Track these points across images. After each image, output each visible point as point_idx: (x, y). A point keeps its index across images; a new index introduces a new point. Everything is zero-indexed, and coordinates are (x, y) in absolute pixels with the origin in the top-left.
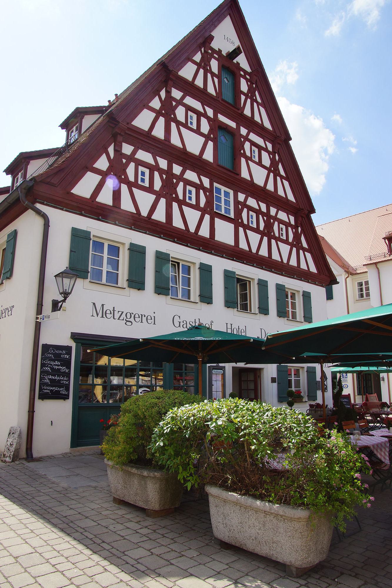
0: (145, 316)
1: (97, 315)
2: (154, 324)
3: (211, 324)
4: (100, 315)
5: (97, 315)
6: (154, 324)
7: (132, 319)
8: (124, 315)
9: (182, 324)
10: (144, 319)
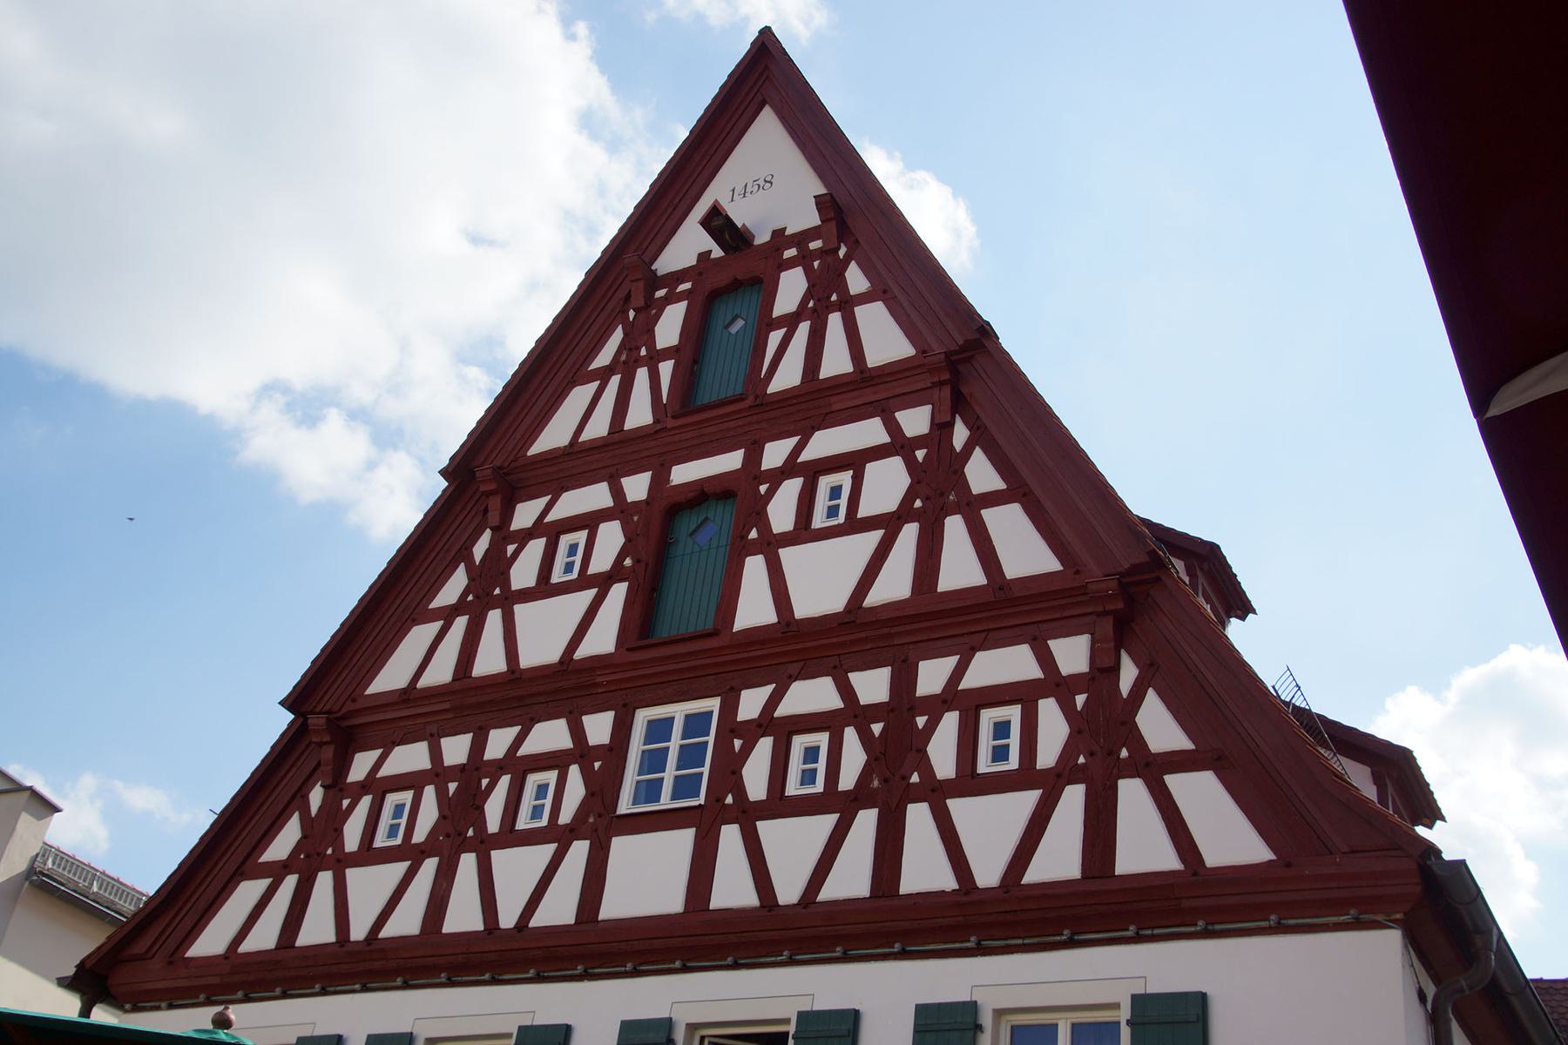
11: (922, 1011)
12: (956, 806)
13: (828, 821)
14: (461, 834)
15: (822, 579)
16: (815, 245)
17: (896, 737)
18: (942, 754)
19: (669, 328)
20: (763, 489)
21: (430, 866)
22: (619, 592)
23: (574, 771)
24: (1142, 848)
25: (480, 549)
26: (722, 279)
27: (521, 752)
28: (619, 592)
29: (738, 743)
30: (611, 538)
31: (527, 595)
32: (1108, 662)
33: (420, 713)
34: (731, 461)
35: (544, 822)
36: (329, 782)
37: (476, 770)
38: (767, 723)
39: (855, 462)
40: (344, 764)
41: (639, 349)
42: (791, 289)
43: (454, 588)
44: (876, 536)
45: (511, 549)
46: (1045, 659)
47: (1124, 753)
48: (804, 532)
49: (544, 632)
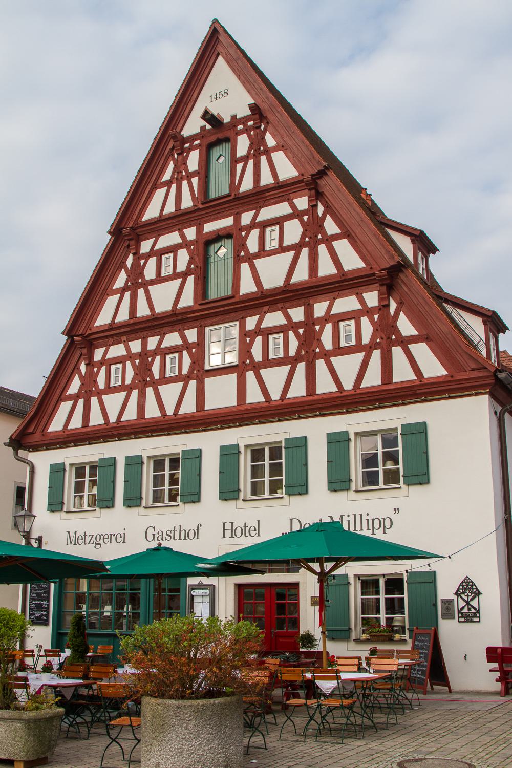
0: (114, 535)
1: (71, 542)
2: (124, 542)
3: (198, 529)
4: (73, 543)
5: (71, 542)
6: (124, 542)
7: (101, 542)
8: (94, 539)
9: (156, 536)
10: (113, 538)
11: (329, 435)
12: (333, 360)
13: (287, 368)
14: (144, 380)
15: (273, 272)
16: (251, 123)
17: (309, 333)
18: (327, 341)
19: (193, 161)
20: (243, 234)
21: (135, 393)
22: (191, 279)
23: (185, 353)
24: (402, 373)
25: (129, 261)
26: (213, 139)
27: (162, 346)
28: (191, 279)
29: (248, 339)
30: (183, 257)
31: (152, 282)
32: (385, 303)
34: (228, 222)
35: (177, 373)
36: (87, 362)
37: (144, 354)
38: (258, 331)
39: (279, 221)
40: (91, 356)
41: (181, 172)
42: (243, 144)
43: (121, 280)
44: (292, 253)
45: (142, 262)
46: (362, 301)
47: (394, 337)
48: (263, 252)
49: (164, 297)
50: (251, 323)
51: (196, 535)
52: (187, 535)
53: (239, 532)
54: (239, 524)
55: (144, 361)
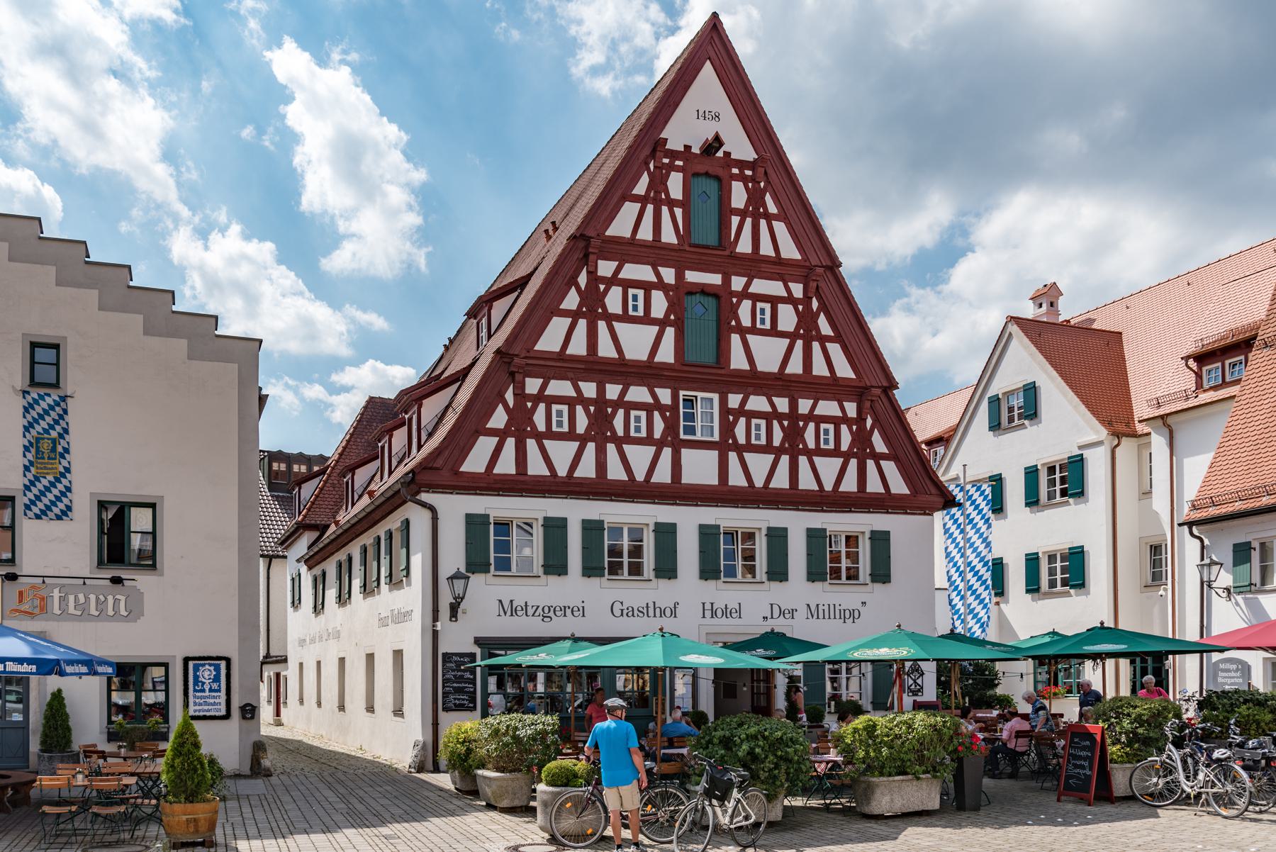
24: (874, 486)
33: (560, 365)
46: (843, 409)
49: (636, 342)
50: (734, 400)
51: (674, 613)
52: (663, 613)
53: (719, 613)
54: (719, 605)
55: (601, 412)
